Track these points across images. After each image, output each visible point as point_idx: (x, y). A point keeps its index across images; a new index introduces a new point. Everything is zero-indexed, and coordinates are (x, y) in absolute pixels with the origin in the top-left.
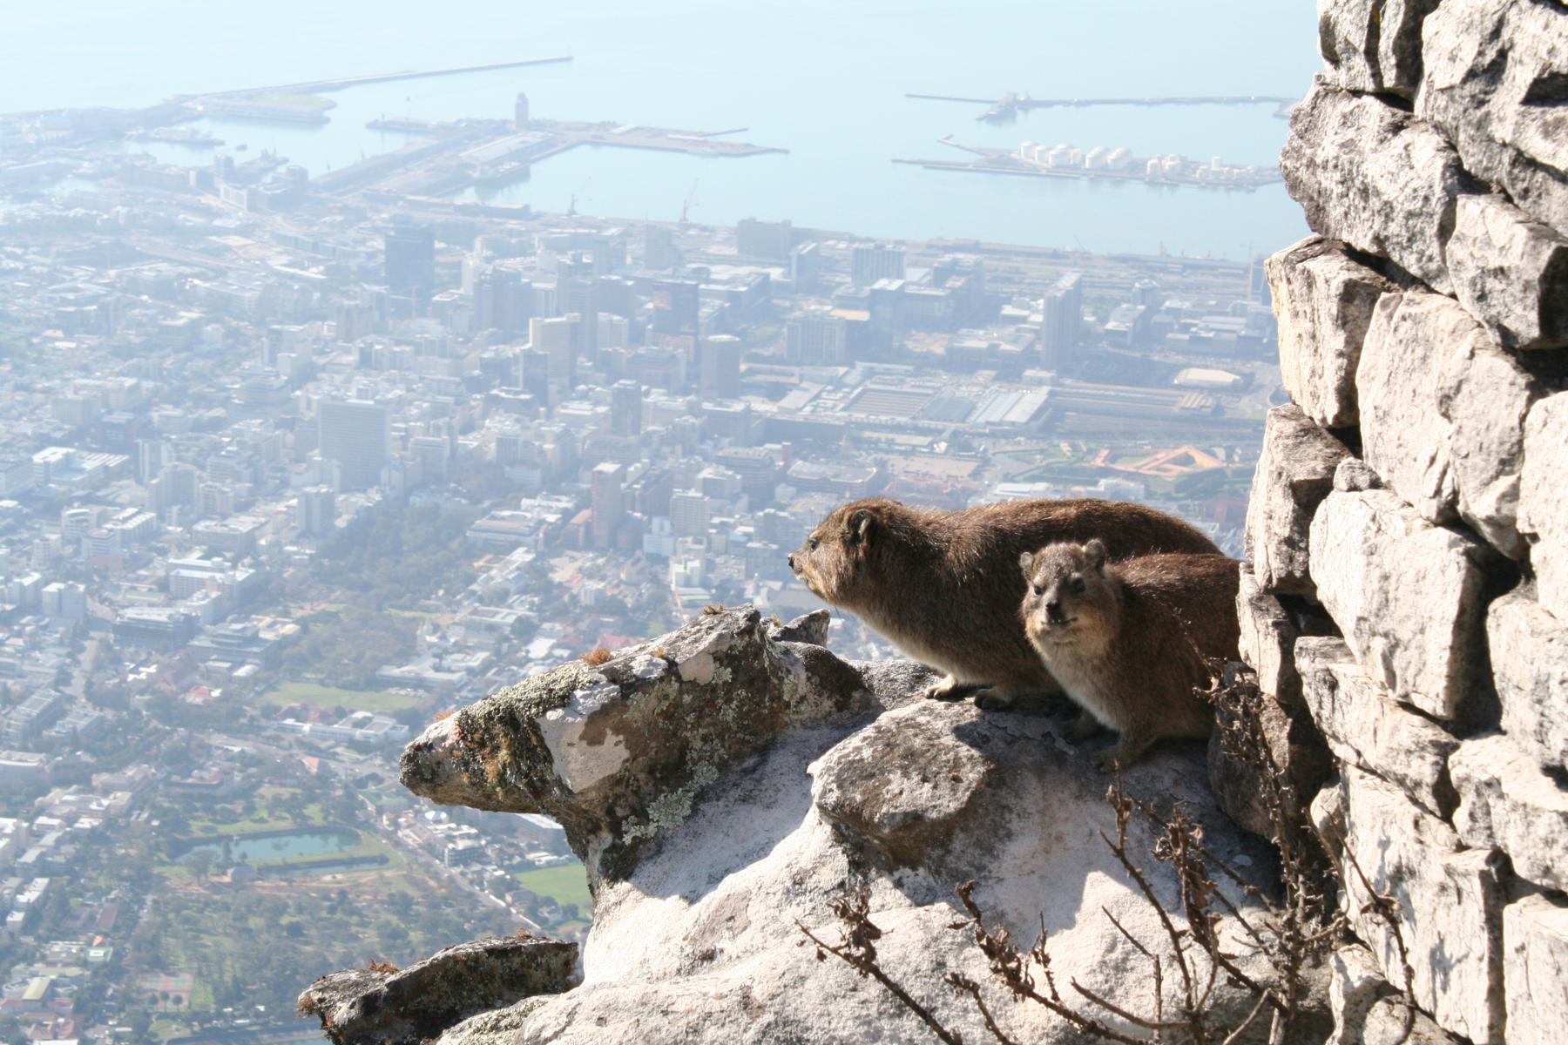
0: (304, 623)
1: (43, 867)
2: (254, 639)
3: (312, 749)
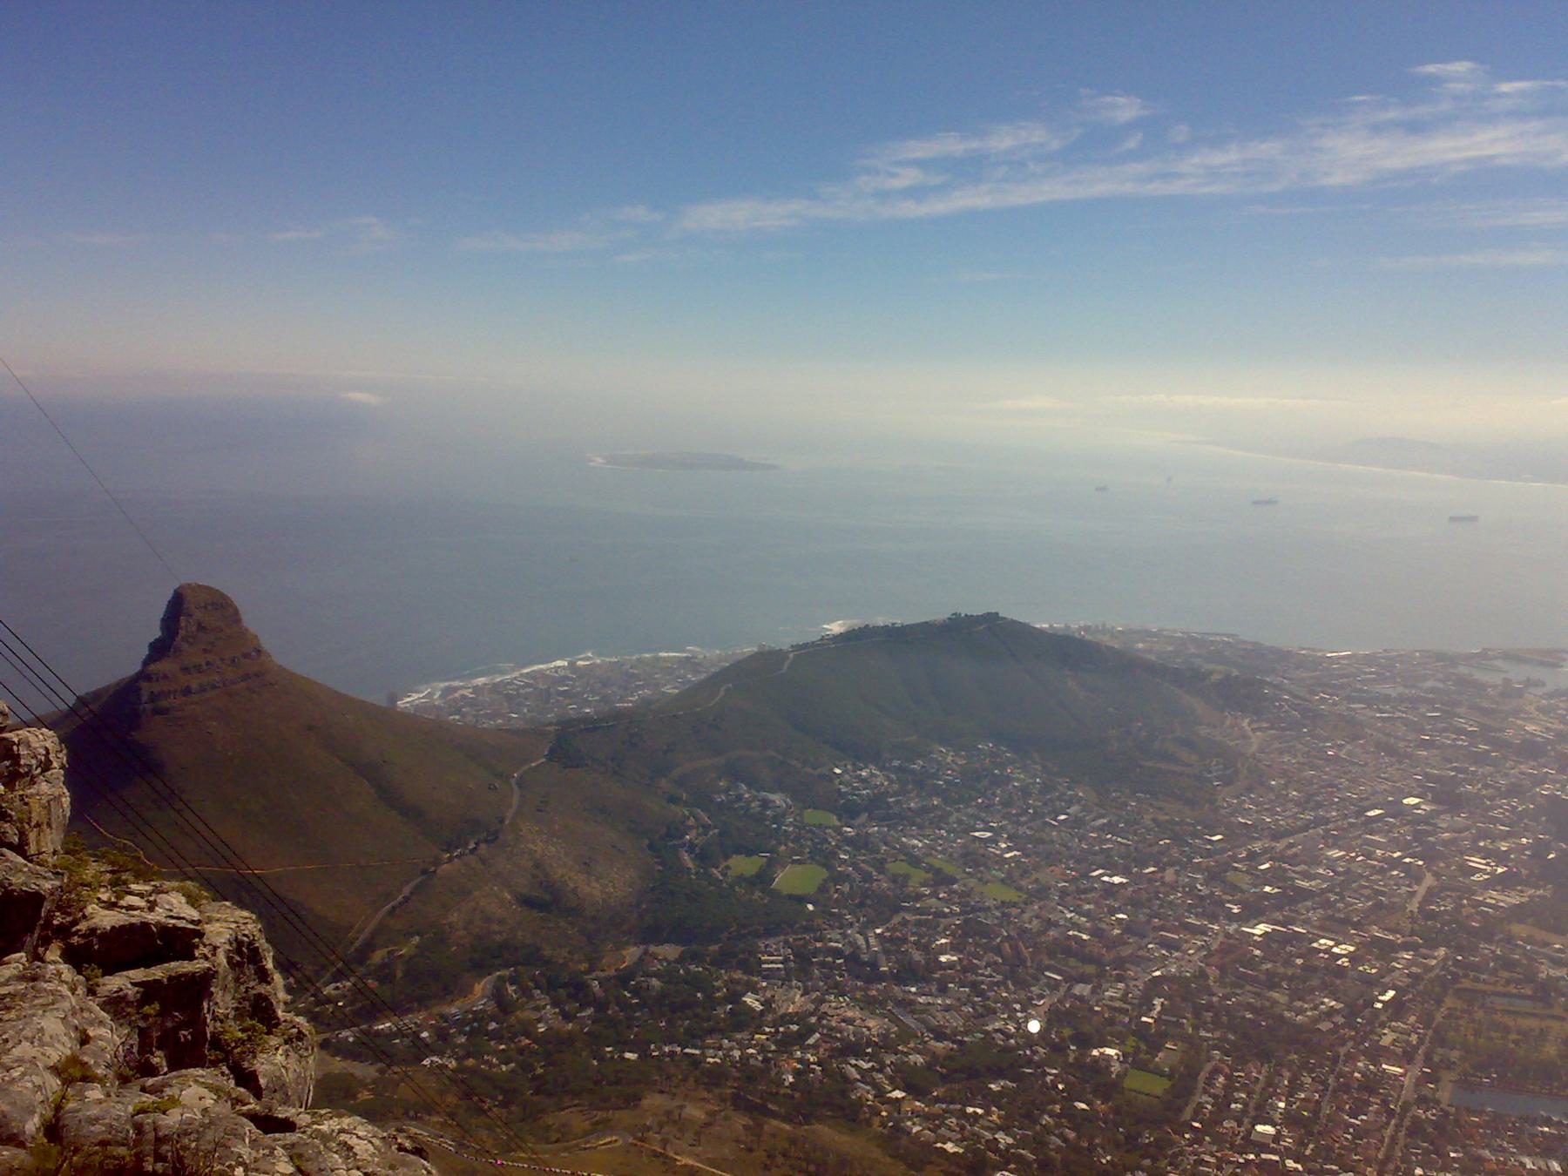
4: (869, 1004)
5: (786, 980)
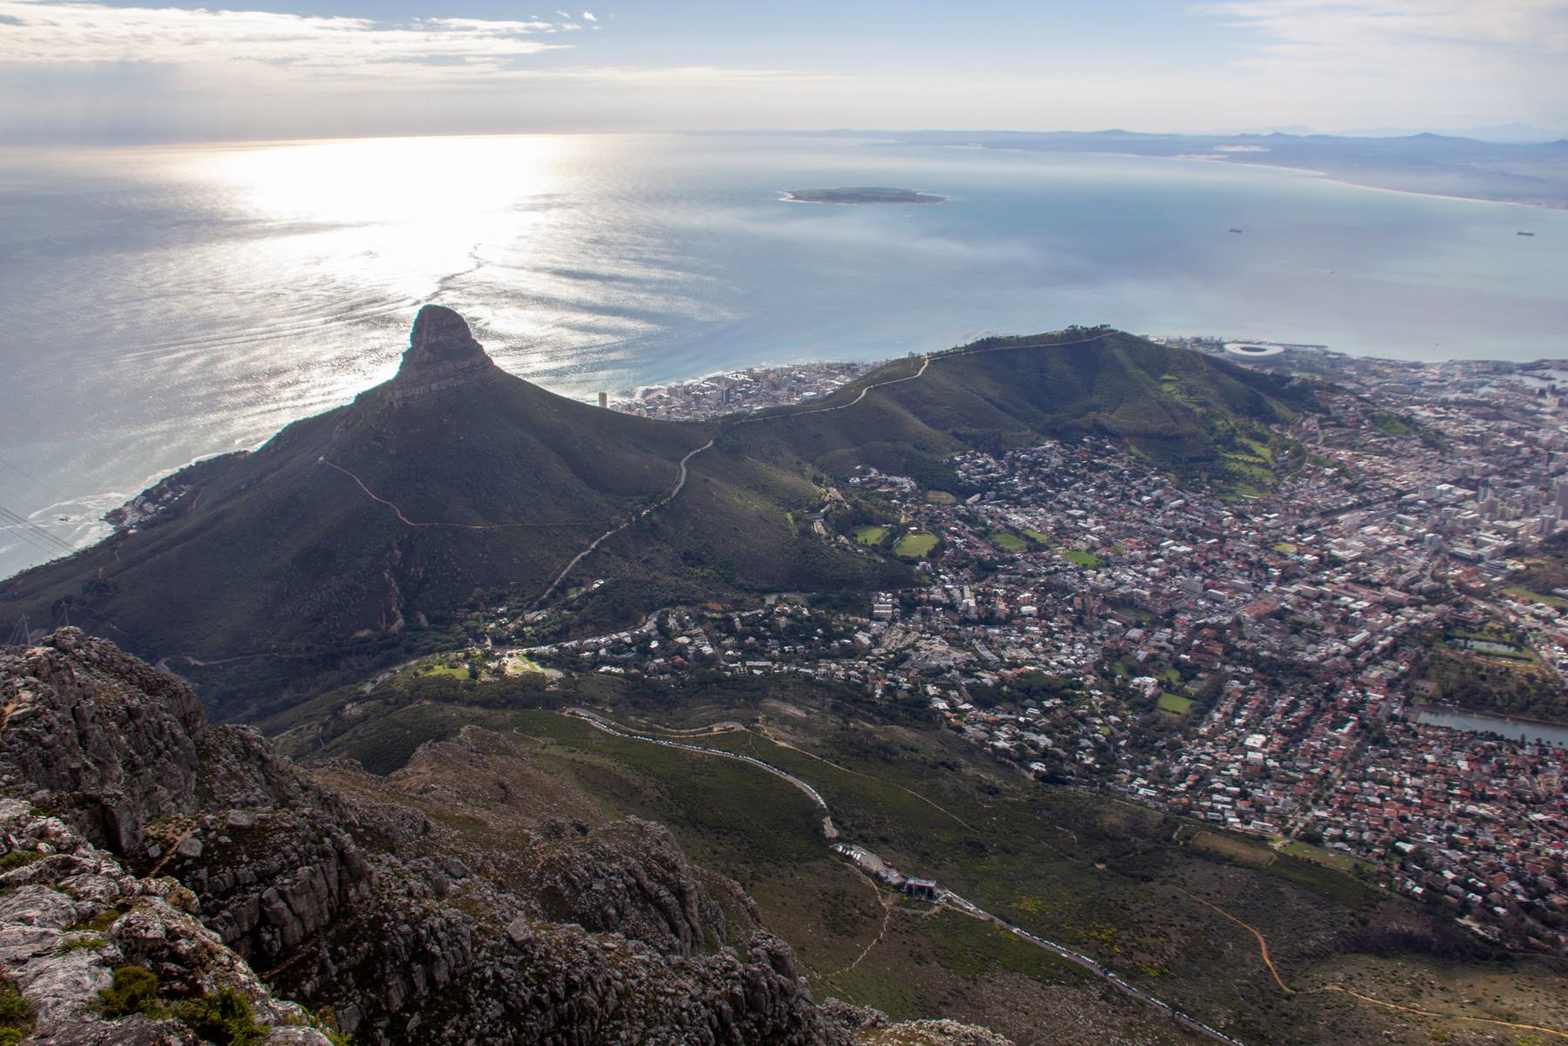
0: (1528, 566)
1: (1393, 635)
2: (1504, 568)
3: (1514, 612)
4: (956, 642)
5: (893, 620)
